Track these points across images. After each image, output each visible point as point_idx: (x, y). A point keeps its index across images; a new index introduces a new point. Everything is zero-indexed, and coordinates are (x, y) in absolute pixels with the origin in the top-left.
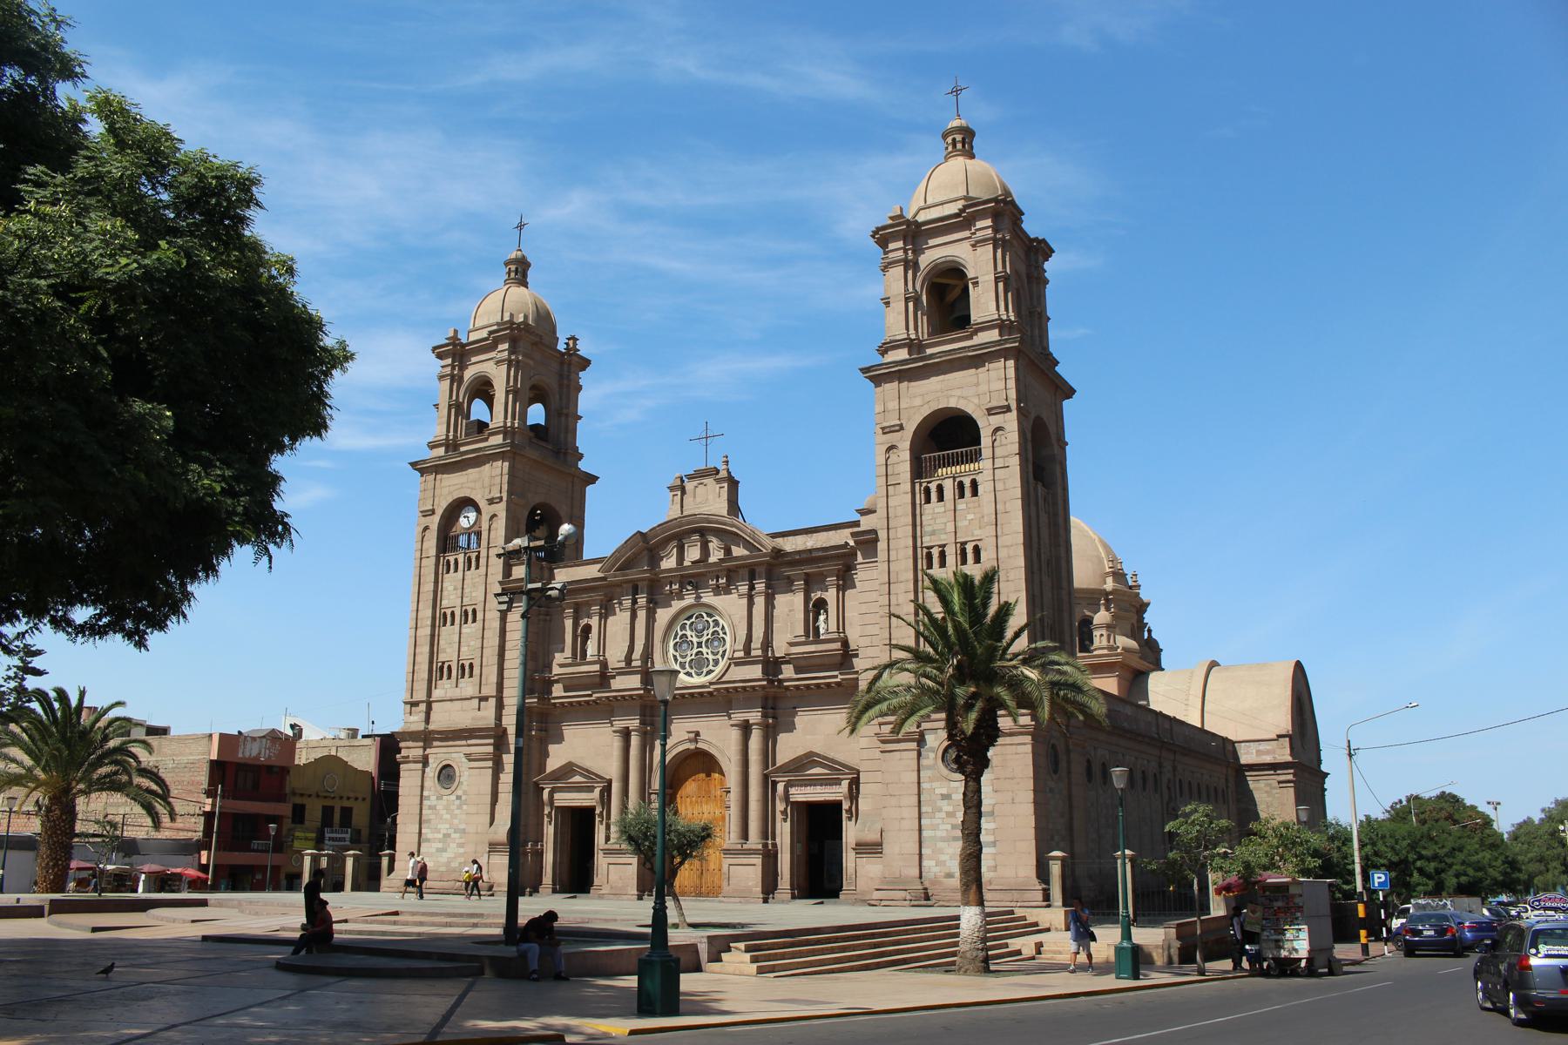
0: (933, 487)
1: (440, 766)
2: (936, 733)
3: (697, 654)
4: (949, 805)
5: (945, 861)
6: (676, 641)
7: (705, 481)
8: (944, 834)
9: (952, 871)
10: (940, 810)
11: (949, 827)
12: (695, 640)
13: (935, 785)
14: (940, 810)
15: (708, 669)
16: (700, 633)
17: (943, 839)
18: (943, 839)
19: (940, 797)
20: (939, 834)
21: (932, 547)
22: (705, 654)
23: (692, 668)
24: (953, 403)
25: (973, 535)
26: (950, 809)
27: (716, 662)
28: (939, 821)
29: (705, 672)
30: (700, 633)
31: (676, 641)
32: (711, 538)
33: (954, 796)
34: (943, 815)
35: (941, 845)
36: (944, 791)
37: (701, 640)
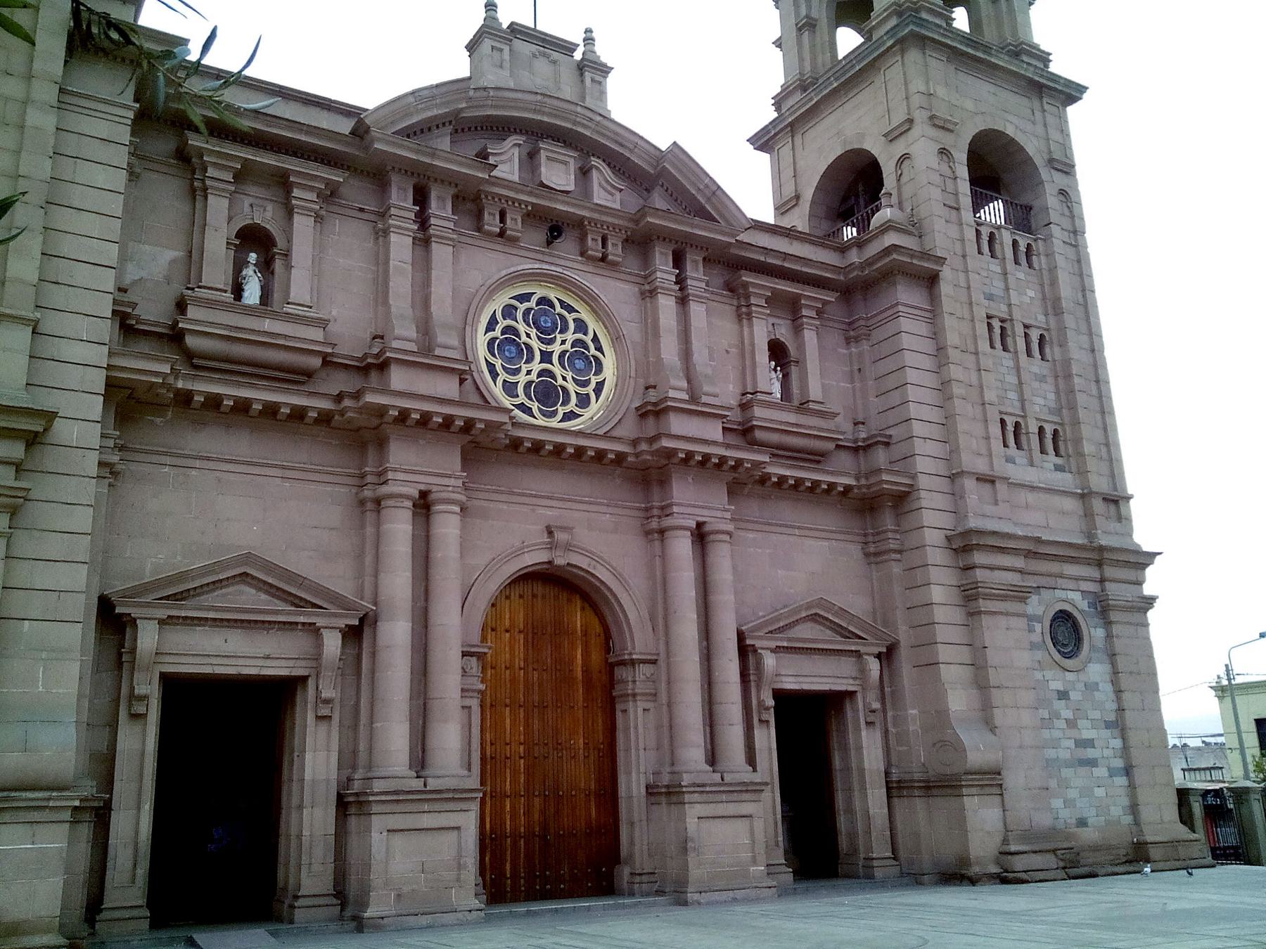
3: (518, 371)
5: (1074, 800)
11: (1071, 744)
12: (536, 345)
13: (1049, 674)
14: (1058, 717)
15: (568, 409)
17: (1069, 764)
18: (1069, 764)
20: (1064, 755)
22: (569, 378)
23: (530, 399)
24: (1010, 131)
25: (1036, 319)
27: (584, 401)
29: (560, 416)
32: (595, 161)
33: (1073, 695)
34: (1062, 724)
35: (1067, 773)
37: (550, 348)
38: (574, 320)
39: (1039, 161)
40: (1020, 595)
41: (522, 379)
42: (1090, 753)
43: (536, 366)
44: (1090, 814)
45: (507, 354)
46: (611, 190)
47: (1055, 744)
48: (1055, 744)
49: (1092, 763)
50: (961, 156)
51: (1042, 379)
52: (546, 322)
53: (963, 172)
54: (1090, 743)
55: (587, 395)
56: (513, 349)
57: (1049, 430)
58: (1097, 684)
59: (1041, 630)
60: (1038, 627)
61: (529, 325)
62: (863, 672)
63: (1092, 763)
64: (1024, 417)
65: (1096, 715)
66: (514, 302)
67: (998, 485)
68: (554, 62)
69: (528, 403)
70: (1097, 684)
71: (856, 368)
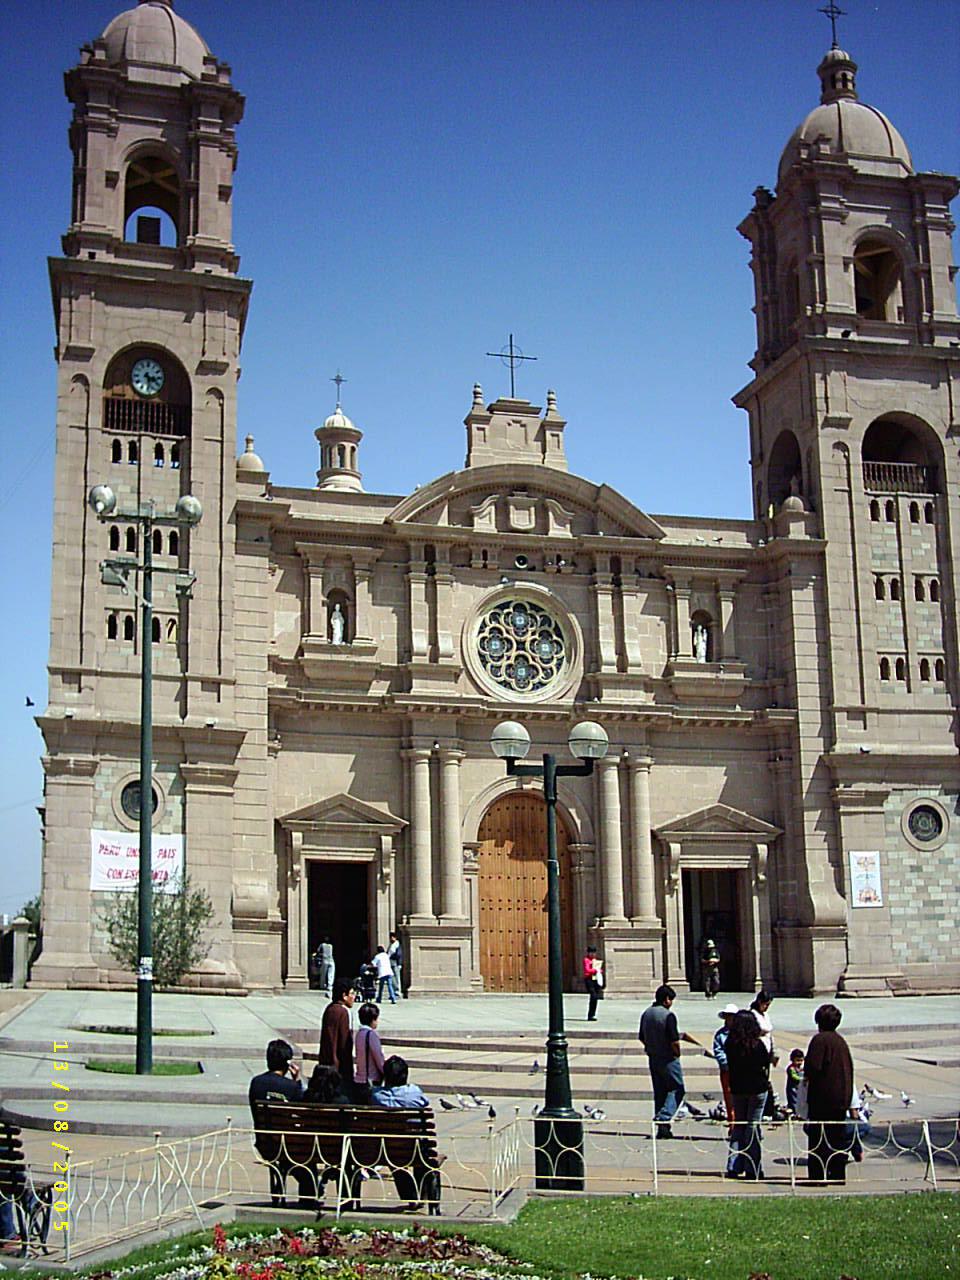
0: (882, 502)
1: (126, 782)
2: (902, 795)
4: (919, 878)
6: (482, 635)
7: (524, 420)
8: (916, 912)
9: (926, 954)
10: (909, 884)
13: (903, 854)
16: (520, 631)
17: (913, 918)
19: (909, 869)
20: (910, 911)
21: (882, 574)
25: (930, 568)
26: (921, 883)
28: (909, 897)
30: (520, 631)
31: (482, 635)
32: (550, 501)
33: (924, 869)
35: (911, 924)
36: (913, 862)
38: (541, 617)
39: (941, 431)
40: (879, 798)
41: (504, 663)
42: (938, 910)
43: (514, 653)
44: (933, 954)
45: (493, 647)
46: (561, 523)
47: (905, 904)
48: (905, 904)
49: (942, 917)
50: (856, 447)
51: (931, 618)
52: (520, 621)
53: (857, 458)
54: (940, 903)
55: (551, 669)
56: (498, 643)
57: (932, 661)
58: (952, 859)
59: (901, 822)
60: (898, 820)
61: (508, 624)
62: (755, 854)
63: (942, 917)
64: (907, 654)
65: (949, 882)
66: (497, 611)
67: (868, 715)
68: (523, 426)
69: (508, 679)
70: (952, 859)
71: (769, 623)
